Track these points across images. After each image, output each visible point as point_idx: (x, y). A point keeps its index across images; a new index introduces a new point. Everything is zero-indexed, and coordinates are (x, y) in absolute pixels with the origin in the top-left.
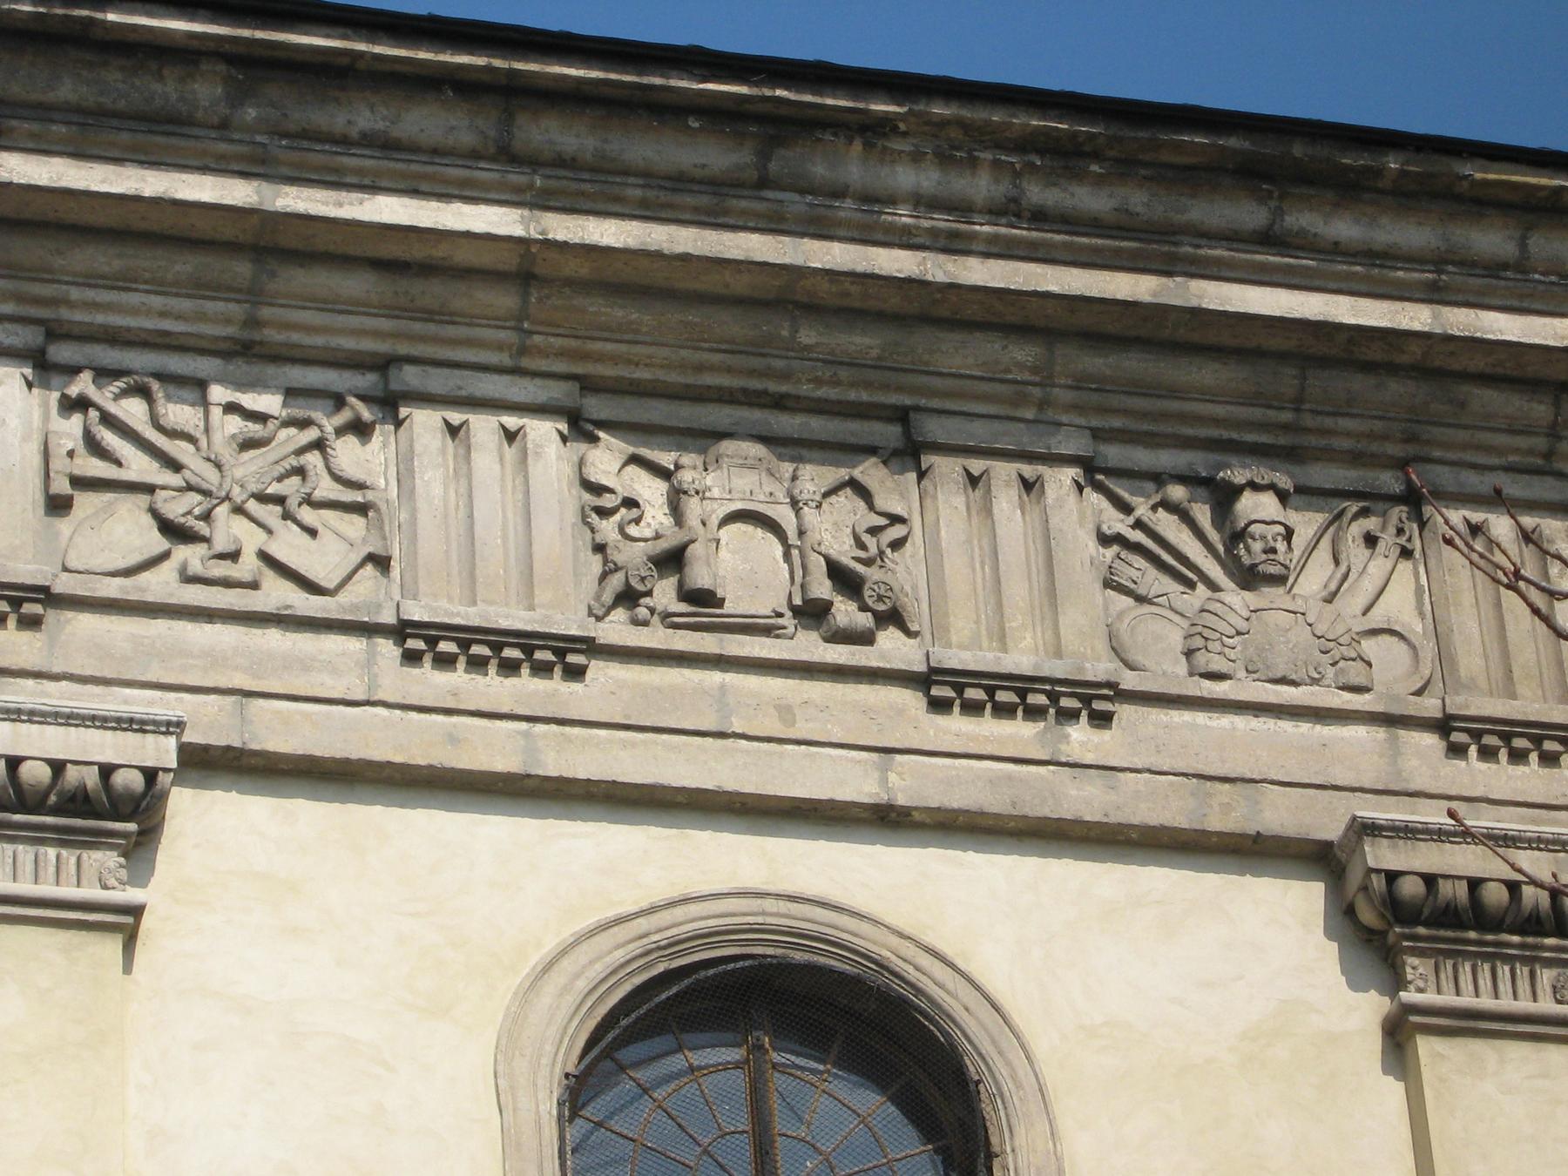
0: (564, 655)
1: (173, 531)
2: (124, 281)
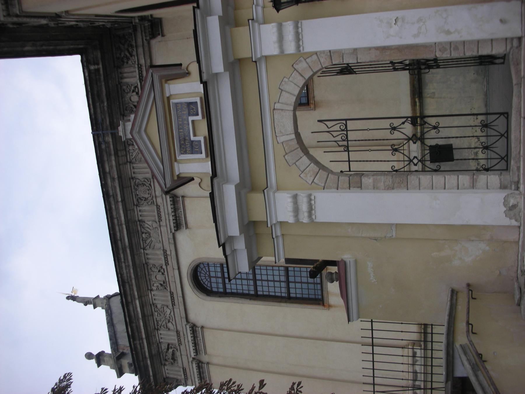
0: (172, 294)
1: (169, 322)
2: (150, 325)
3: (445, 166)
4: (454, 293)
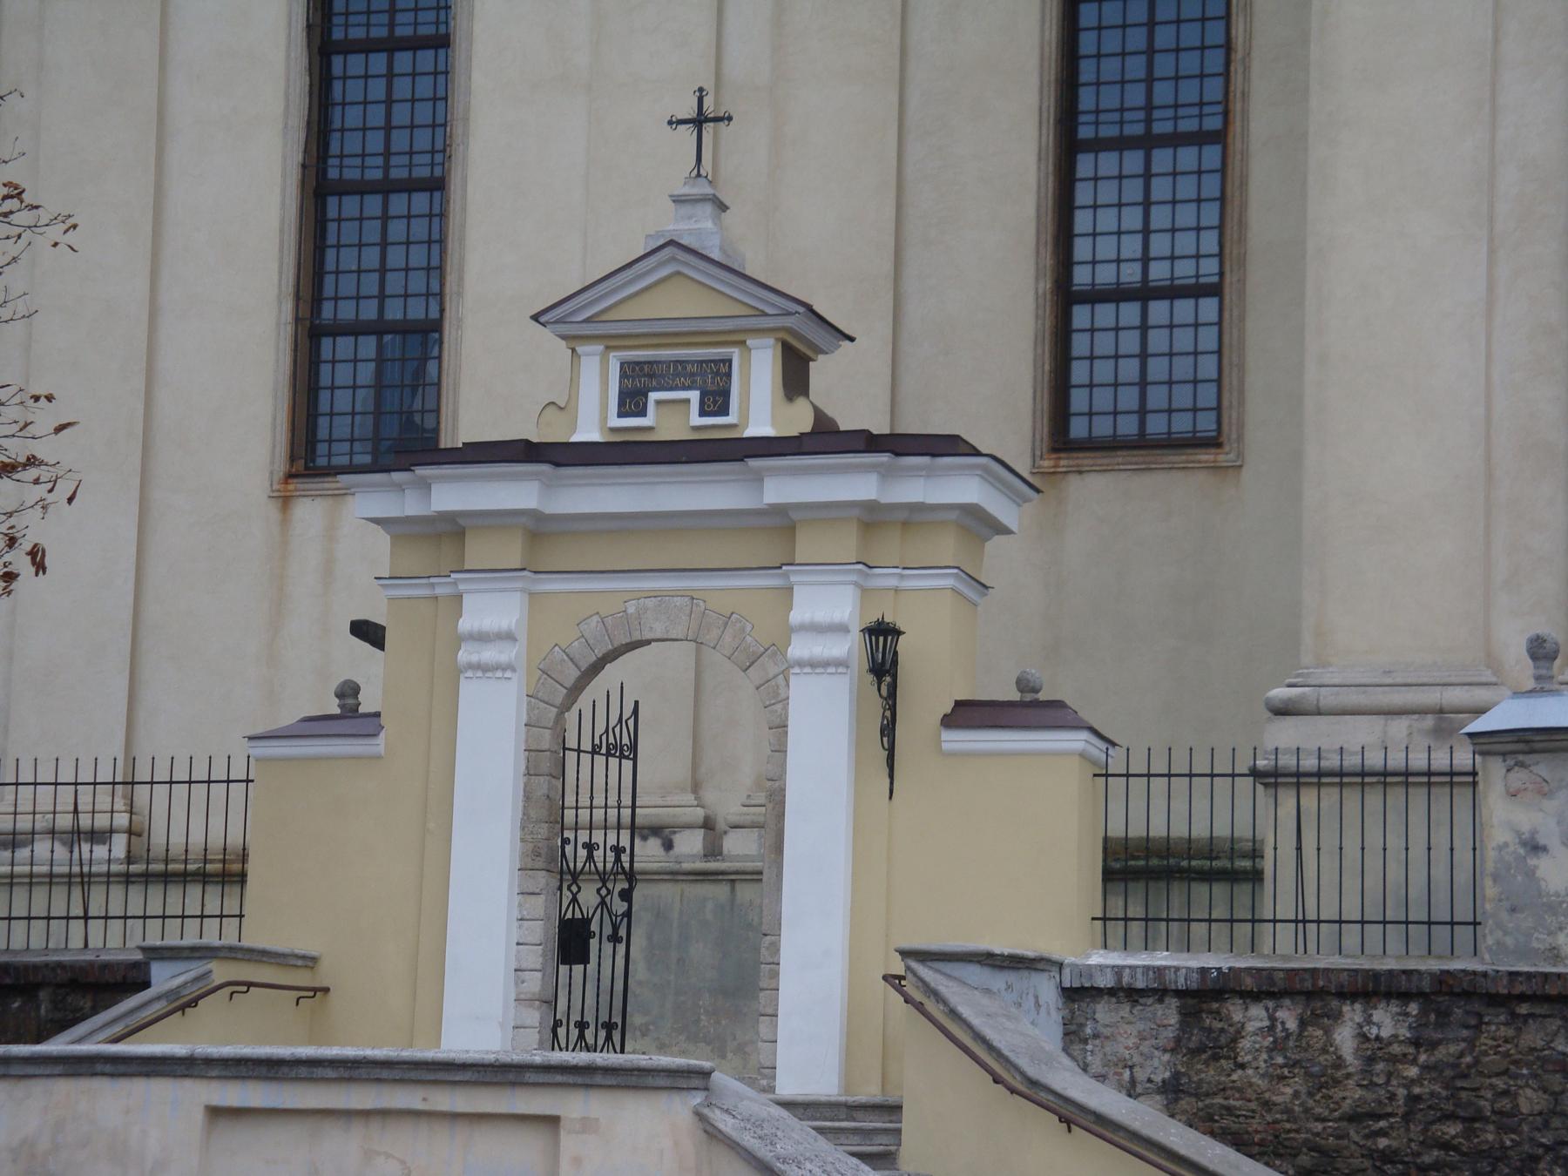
4: (310, 962)
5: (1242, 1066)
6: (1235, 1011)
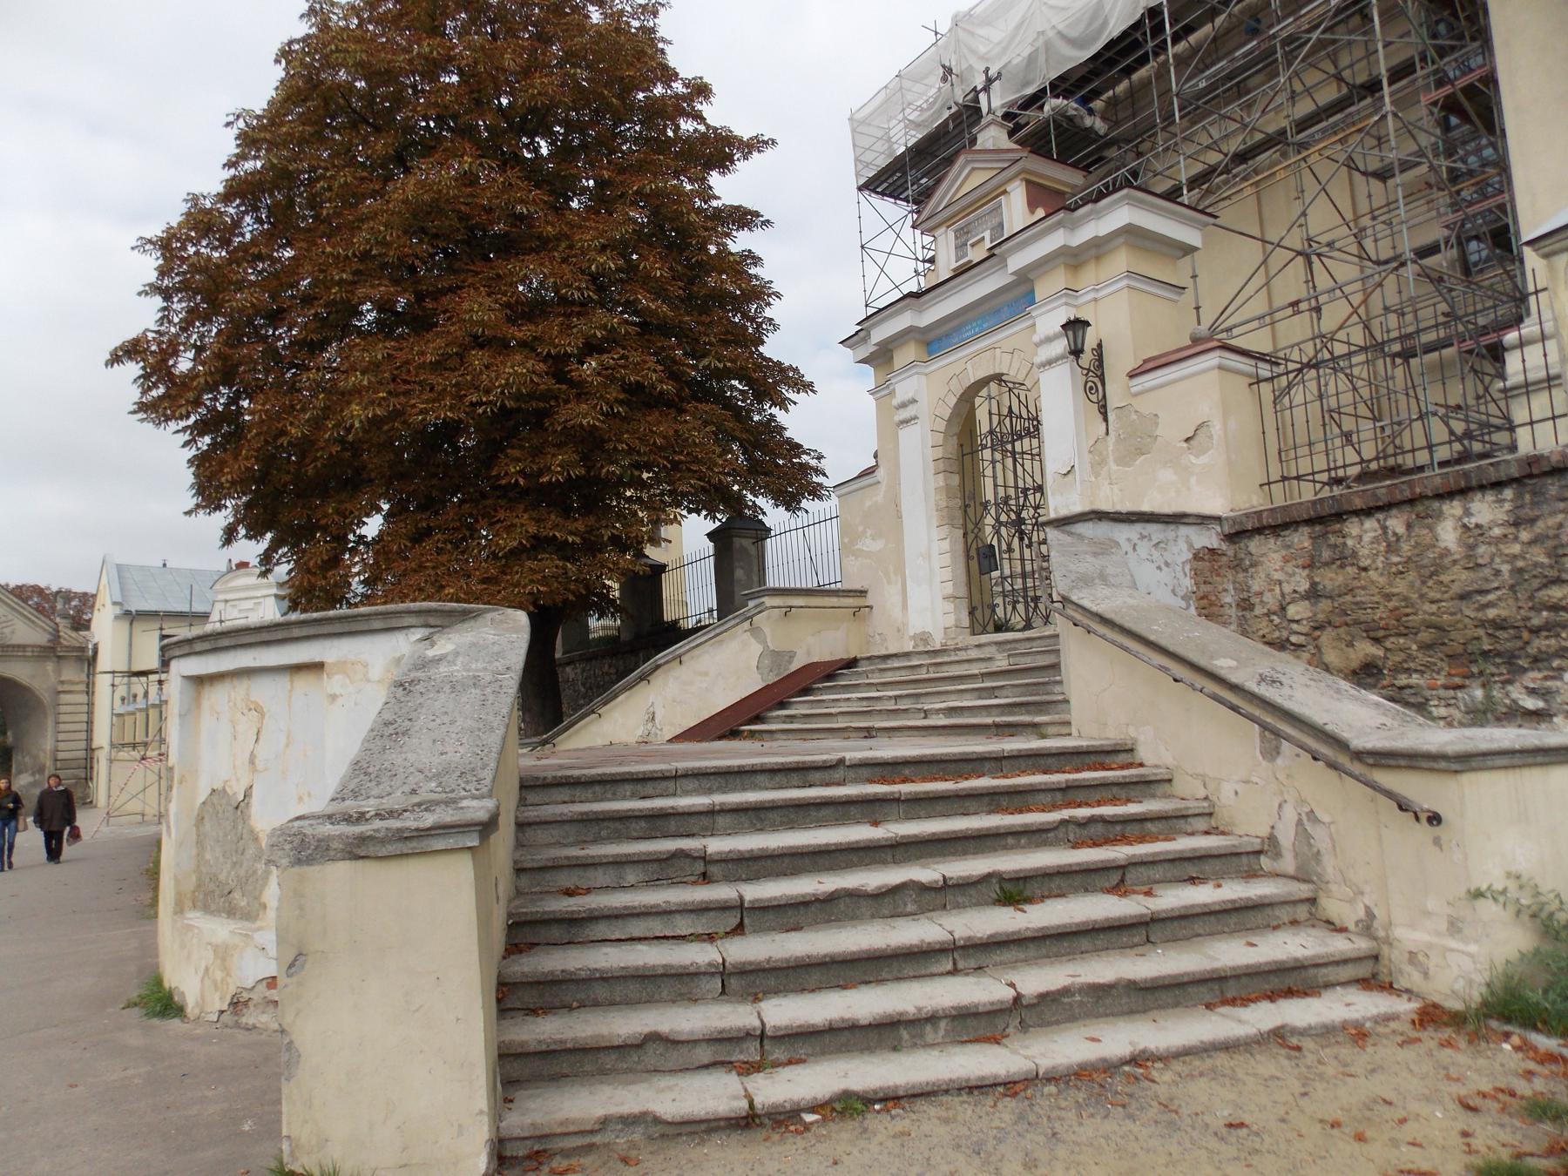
3: (974, 564)
4: (862, 593)
5: (1365, 569)
6: (1353, 527)
